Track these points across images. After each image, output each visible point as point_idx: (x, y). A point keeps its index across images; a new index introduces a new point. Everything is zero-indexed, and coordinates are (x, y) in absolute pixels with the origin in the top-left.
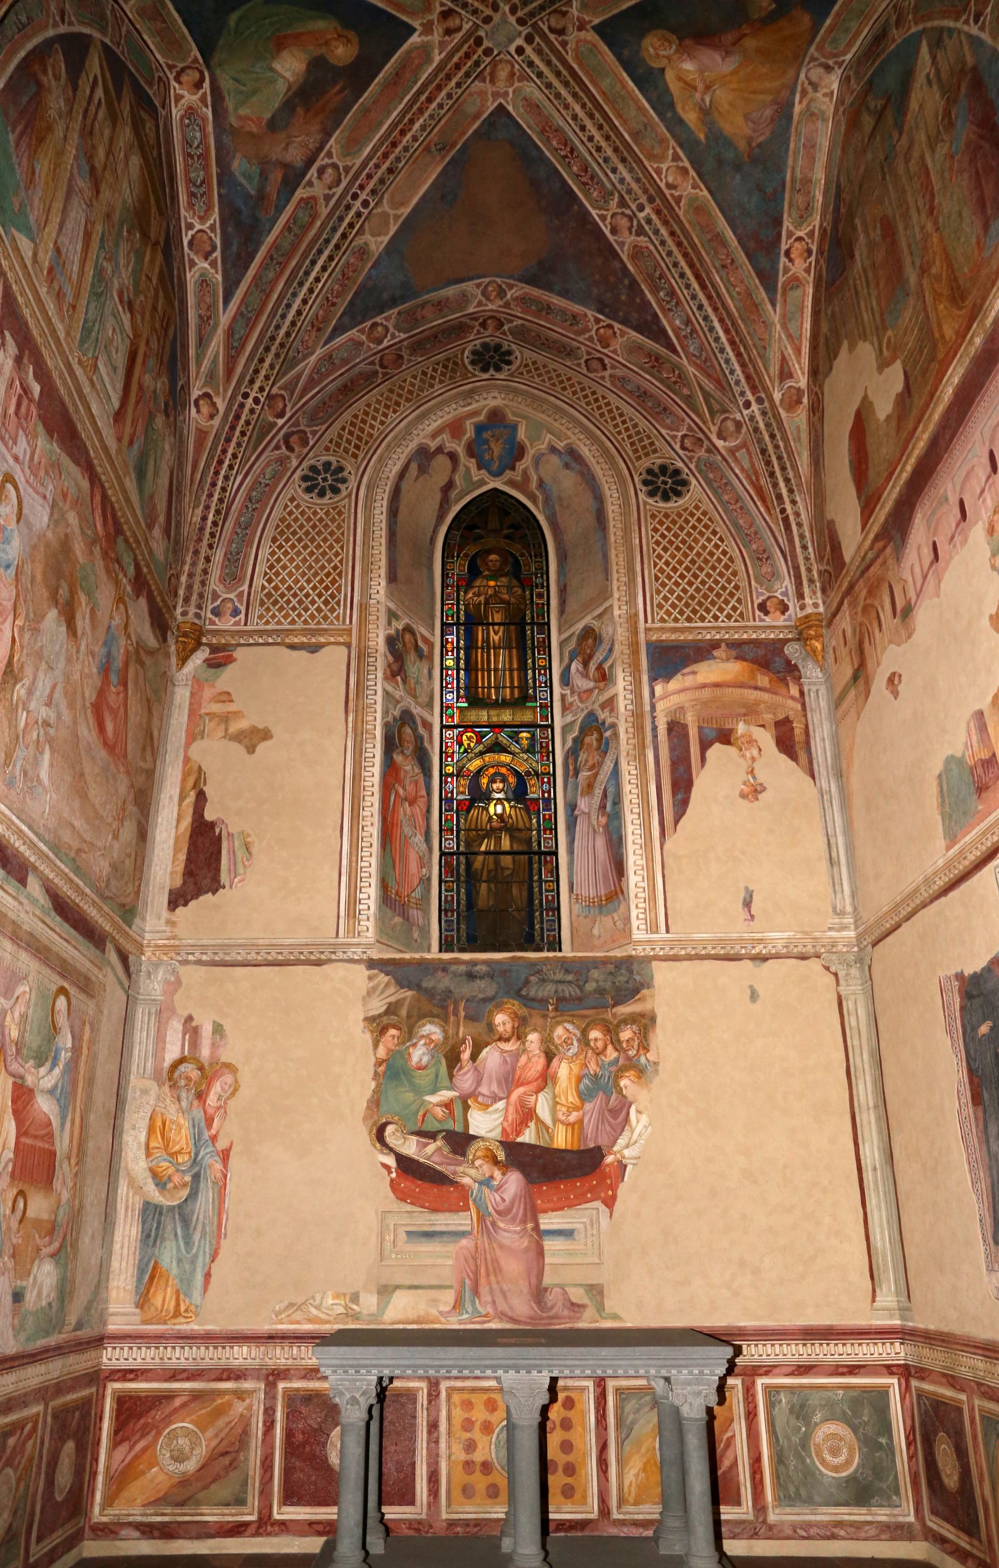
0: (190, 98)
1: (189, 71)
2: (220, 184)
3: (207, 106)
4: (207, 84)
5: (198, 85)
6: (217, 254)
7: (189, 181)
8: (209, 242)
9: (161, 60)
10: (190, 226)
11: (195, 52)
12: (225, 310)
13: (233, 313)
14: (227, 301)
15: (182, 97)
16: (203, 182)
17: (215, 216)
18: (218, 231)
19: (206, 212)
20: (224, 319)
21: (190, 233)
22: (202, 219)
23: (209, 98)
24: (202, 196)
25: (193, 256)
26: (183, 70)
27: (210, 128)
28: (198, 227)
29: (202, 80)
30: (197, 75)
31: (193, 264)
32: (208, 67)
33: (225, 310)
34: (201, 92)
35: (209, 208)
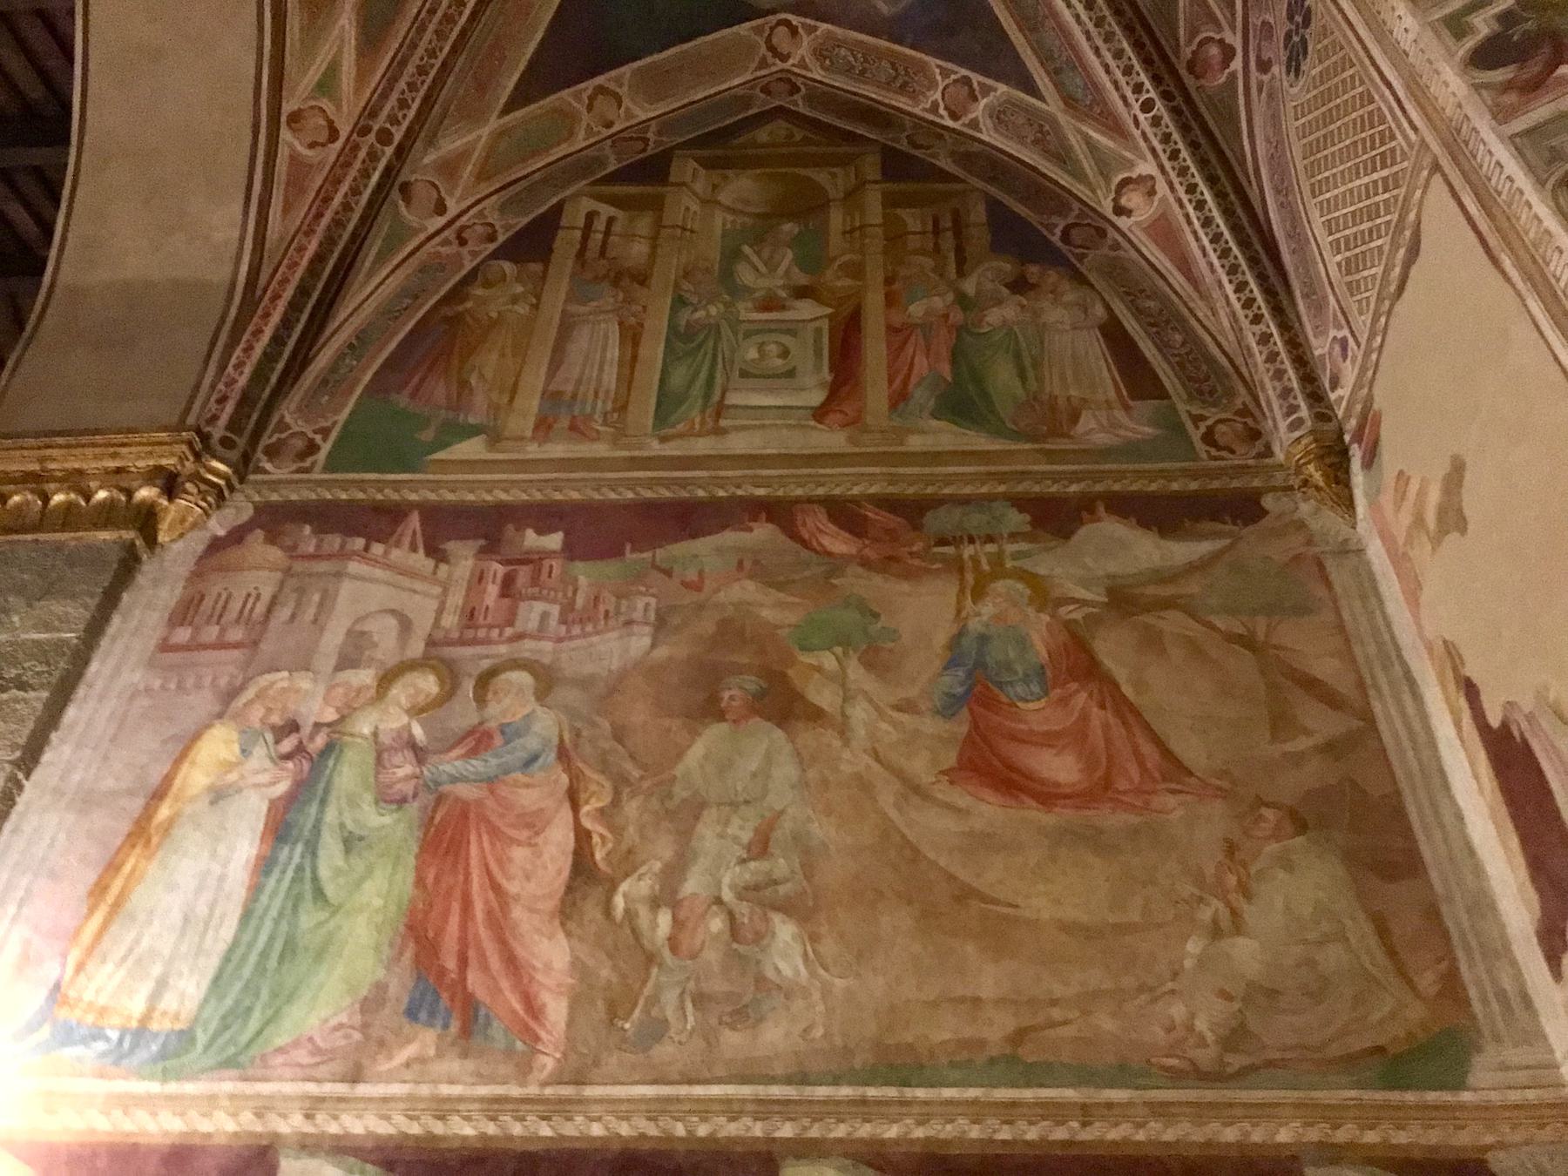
0: (803, 50)
1: (775, 41)
2: (900, 43)
3: (815, 28)
4: (795, 20)
5: (794, 31)
6: (976, 78)
7: (887, 85)
8: (959, 86)
9: (748, 76)
10: (934, 108)
11: (744, 29)
12: (1041, 98)
13: (1050, 85)
14: (1033, 90)
15: (803, 57)
16: (893, 65)
17: (933, 62)
18: (950, 65)
19: (925, 76)
20: (1052, 105)
21: (942, 111)
22: (933, 84)
23: (808, 21)
24: (907, 73)
25: (966, 120)
26: (772, 48)
27: (839, 31)
28: (938, 96)
29: (787, 23)
30: (782, 29)
31: (974, 124)
32: (773, 12)
33: (1041, 98)
34: (800, 30)
35: (923, 68)
